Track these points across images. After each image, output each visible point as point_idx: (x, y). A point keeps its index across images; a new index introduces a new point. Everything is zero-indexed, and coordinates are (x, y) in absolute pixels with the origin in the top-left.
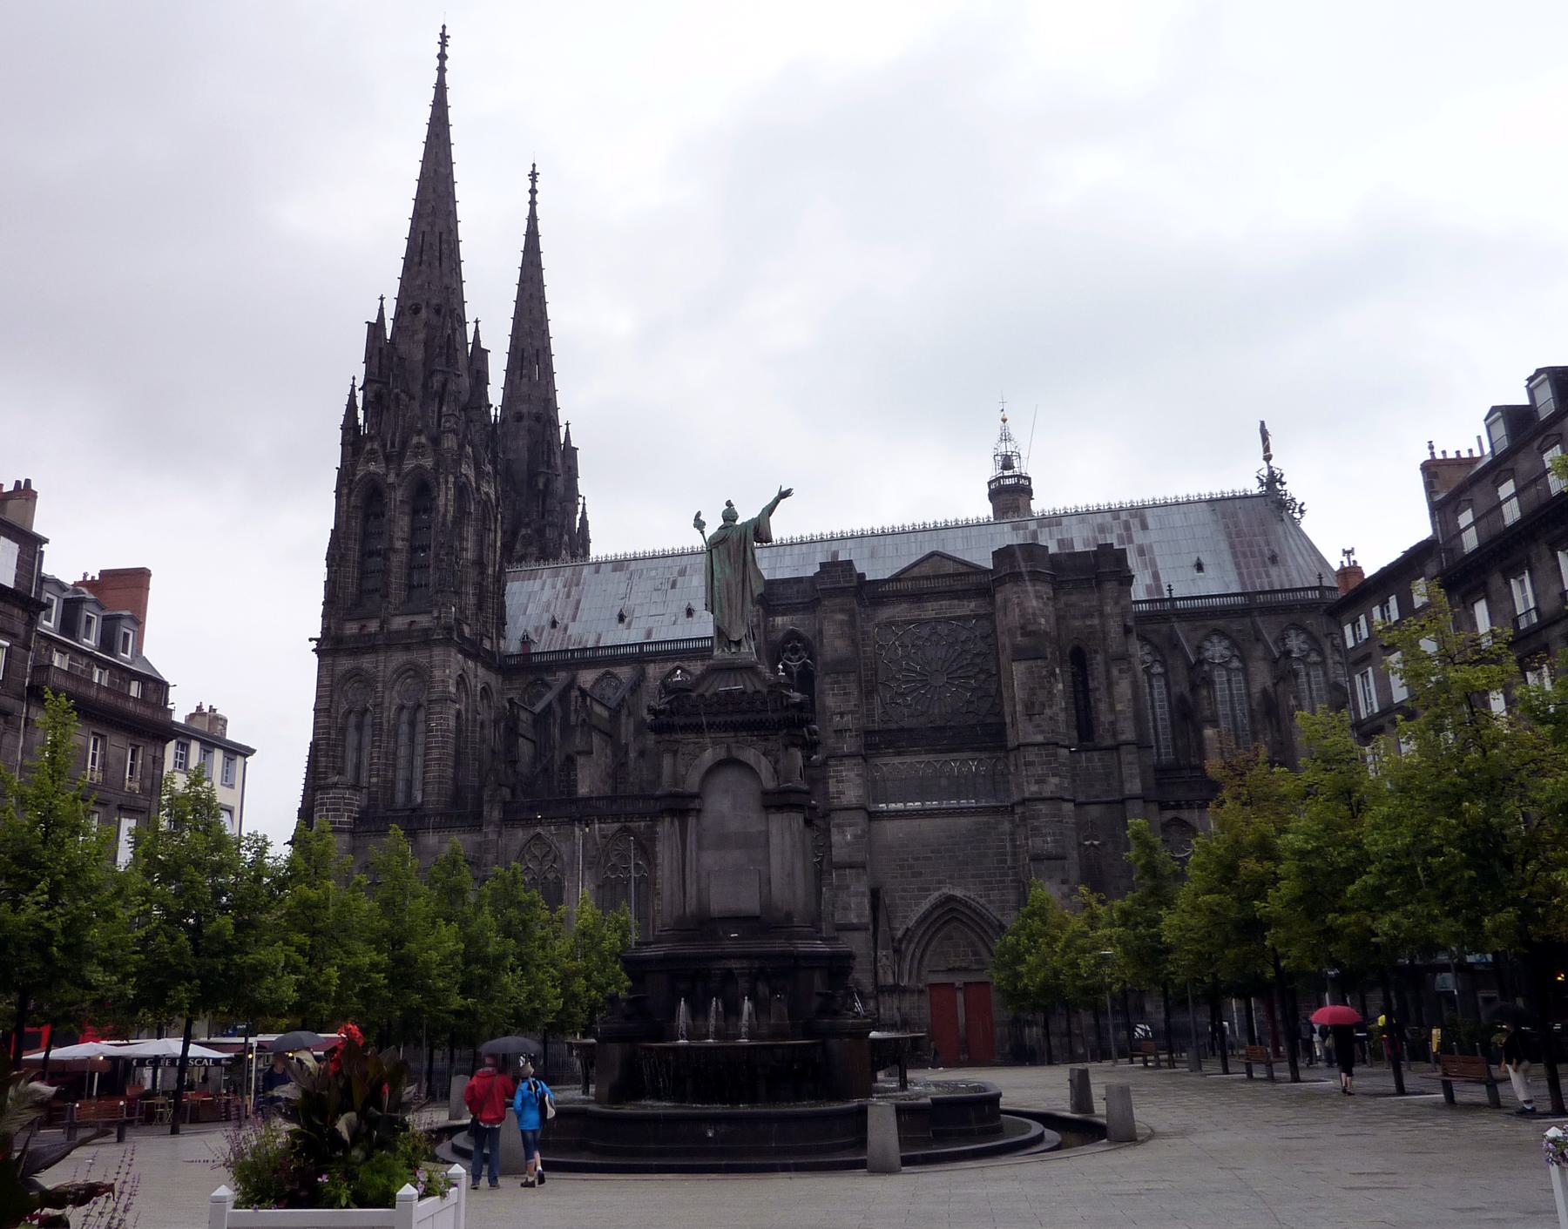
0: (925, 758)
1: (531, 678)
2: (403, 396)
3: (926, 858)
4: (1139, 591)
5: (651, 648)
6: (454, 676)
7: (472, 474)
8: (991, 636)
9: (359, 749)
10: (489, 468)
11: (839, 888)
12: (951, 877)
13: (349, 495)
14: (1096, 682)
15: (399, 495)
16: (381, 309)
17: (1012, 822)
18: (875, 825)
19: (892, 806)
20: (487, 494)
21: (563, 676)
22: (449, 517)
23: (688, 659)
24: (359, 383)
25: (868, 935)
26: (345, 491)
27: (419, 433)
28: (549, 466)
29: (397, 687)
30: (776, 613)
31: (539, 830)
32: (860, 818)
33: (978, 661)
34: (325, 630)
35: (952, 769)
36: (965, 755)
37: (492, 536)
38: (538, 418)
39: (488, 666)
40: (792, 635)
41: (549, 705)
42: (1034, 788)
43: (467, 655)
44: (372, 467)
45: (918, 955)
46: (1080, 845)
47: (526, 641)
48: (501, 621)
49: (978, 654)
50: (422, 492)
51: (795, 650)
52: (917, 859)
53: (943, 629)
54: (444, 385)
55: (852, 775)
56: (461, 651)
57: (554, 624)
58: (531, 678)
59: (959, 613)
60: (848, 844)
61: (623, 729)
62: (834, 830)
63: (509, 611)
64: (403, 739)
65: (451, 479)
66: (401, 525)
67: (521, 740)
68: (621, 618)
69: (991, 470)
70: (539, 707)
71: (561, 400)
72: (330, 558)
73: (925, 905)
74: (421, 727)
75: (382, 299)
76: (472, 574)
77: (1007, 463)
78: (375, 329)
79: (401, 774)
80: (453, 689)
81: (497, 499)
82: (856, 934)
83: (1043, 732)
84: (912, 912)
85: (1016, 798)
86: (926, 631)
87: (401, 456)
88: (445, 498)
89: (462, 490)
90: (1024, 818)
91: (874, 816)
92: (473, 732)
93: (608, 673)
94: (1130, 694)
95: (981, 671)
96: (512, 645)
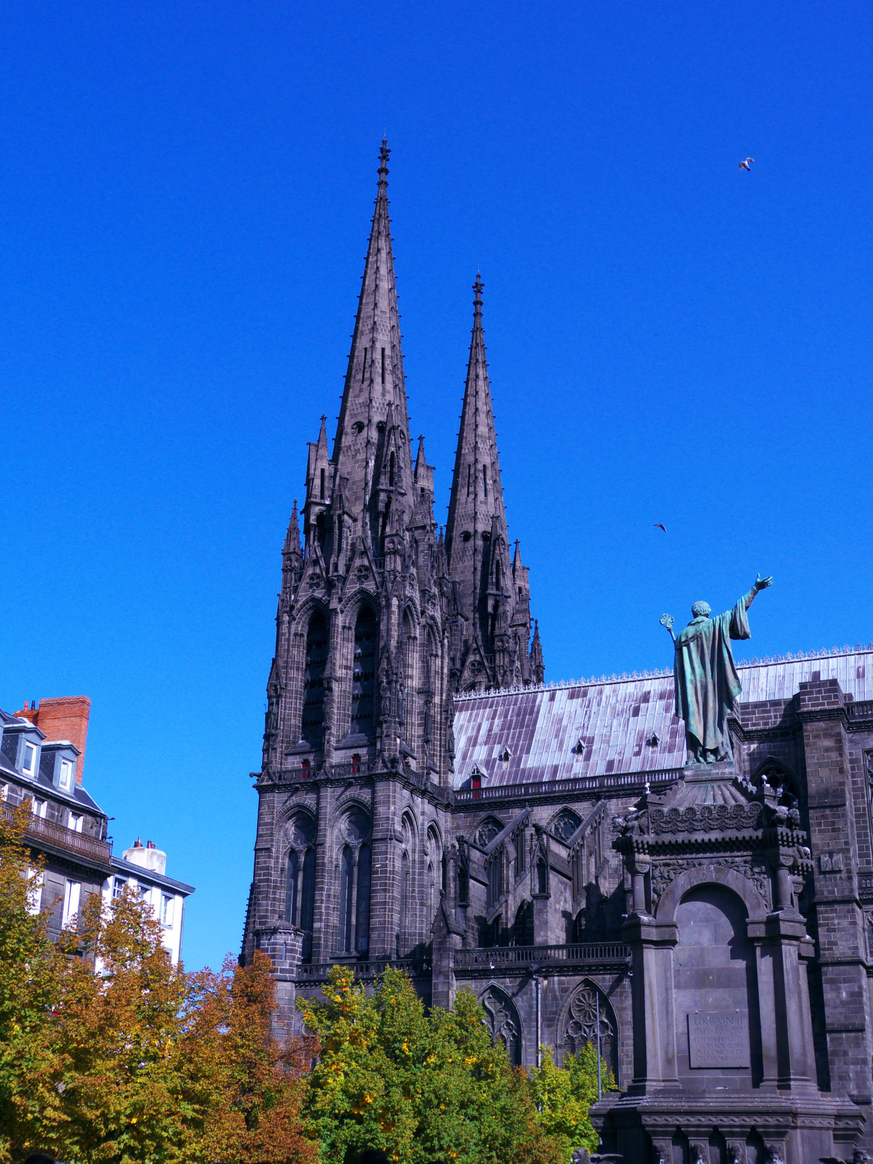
1: (483, 815)
2: (346, 517)
6: (400, 813)
7: (417, 596)
10: (435, 590)
11: (835, 1053)
20: (433, 618)
21: (517, 813)
24: (301, 506)
28: (498, 586)
31: (493, 982)
37: (438, 661)
38: (486, 537)
41: (502, 844)
54: (388, 505)
56: (406, 785)
58: (483, 815)
60: (843, 1004)
61: (584, 872)
66: (344, 654)
70: (491, 846)
80: (398, 827)
81: (443, 623)
87: (344, 580)
89: (406, 614)
92: (421, 874)
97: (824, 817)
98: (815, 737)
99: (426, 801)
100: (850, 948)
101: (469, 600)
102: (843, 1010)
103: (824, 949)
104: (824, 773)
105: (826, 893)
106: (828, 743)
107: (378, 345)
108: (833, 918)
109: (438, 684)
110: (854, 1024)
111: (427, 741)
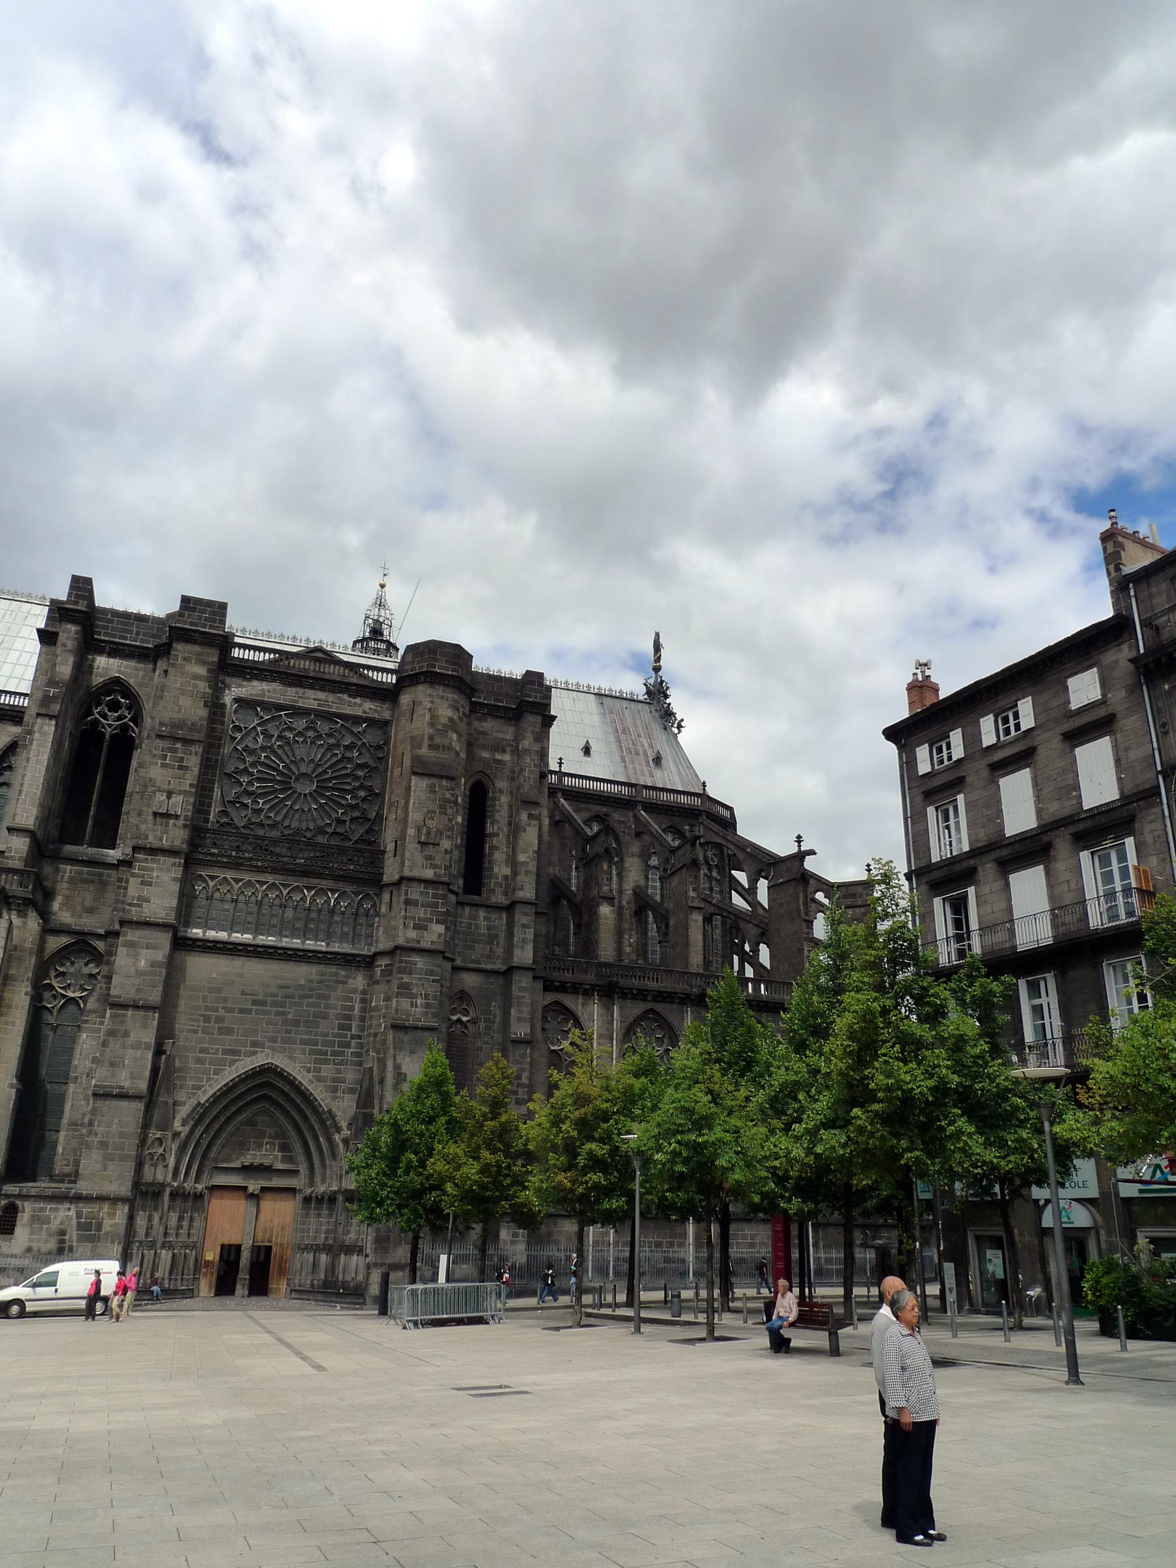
0: (270, 879)
3: (241, 1011)
8: (381, 751)
12: (273, 1040)
14: (497, 824)
17: (371, 977)
18: (180, 955)
19: (211, 934)
25: (140, 1106)
30: (101, 652)
33: (360, 773)
35: (303, 899)
36: (325, 884)
40: (116, 685)
51: (114, 706)
52: (231, 1010)
53: (323, 727)
55: (166, 877)
59: (348, 711)
60: (139, 974)
62: (122, 951)
73: (229, 1074)
82: (124, 1104)
83: (434, 866)
84: (203, 1083)
86: (301, 724)
90: (388, 972)
91: (182, 944)
94: (520, 853)
95: (362, 787)
97: (174, 751)
98: (185, 659)
100: (165, 909)
102: (136, 981)
103: (131, 905)
104: (185, 702)
105: (151, 839)
106: (201, 670)
108: (152, 870)
110: (146, 1000)
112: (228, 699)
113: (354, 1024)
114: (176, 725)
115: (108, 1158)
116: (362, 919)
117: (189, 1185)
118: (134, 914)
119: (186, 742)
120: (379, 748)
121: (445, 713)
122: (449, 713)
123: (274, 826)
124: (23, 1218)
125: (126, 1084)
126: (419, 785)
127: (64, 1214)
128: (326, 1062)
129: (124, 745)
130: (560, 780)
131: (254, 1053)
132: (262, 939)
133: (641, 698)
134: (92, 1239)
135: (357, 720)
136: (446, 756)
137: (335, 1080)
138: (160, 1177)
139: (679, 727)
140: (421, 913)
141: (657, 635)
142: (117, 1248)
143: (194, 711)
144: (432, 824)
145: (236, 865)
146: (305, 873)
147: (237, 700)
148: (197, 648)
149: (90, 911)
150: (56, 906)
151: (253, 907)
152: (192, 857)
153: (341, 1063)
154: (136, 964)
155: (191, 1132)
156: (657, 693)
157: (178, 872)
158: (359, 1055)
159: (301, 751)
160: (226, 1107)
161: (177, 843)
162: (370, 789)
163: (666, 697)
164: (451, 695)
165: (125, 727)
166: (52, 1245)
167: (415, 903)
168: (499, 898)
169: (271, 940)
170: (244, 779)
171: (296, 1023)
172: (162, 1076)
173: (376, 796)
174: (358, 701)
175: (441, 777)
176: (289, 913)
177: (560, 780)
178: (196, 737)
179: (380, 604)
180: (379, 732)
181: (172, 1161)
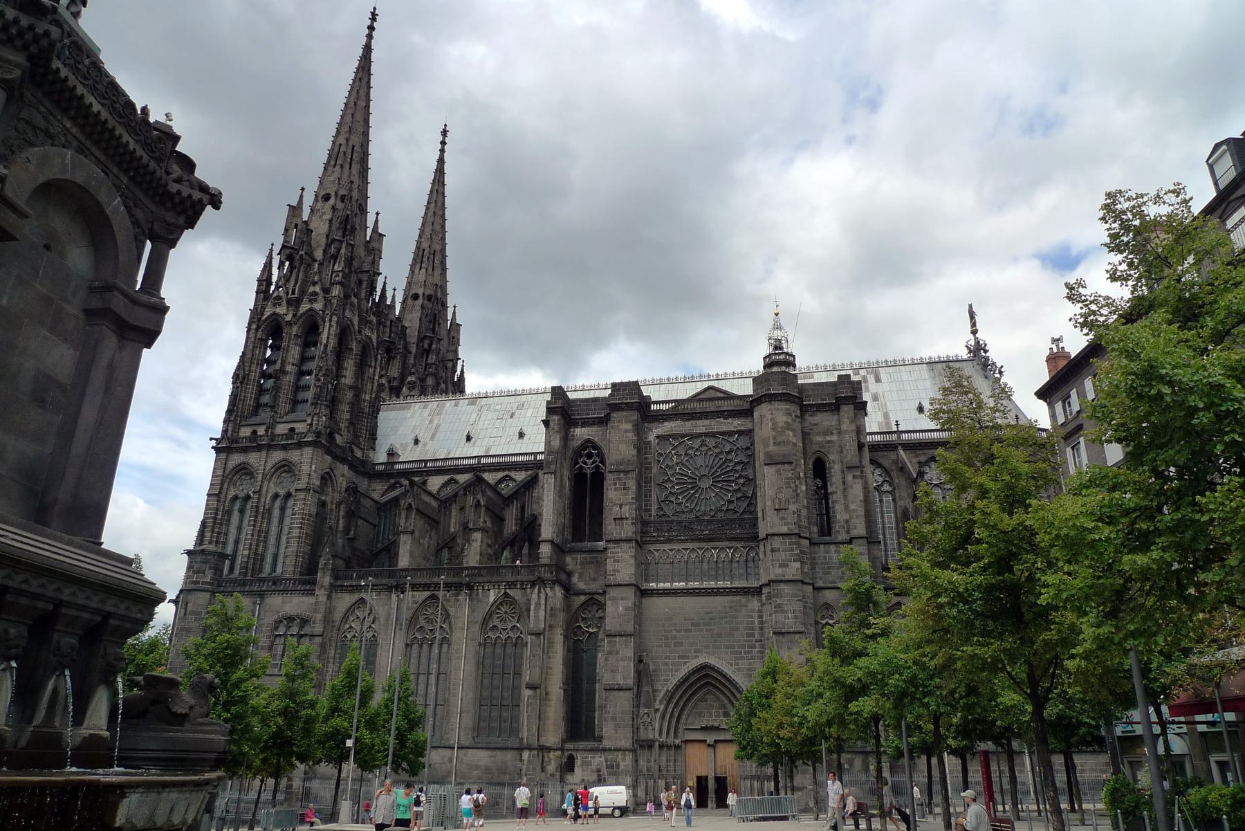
0: (690, 545)
1: (392, 481)
3: (686, 631)
4: (873, 423)
5: (490, 460)
8: (750, 450)
9: (240, 528)
10: (374, 319)
11: (610, 653)
12: (707, 647)
13: (257, 330)
14: (834, 486)
15: (295, 330)
16: (301, 197)
19: (661, 585)
22: (330, 348)
23: (515, 470)
24: (277, 249)
25: (628, 695)
26: (254, 326)
27: (315, 284)
28: (433, 331)
29: (274, 479)
30: (576, 425)
32: (630, 593)
33: (738, 468)
34: (225, 431)
37: (371, 370)
38: (429, 298)
39: (352, 467)
40: (588, 443)
42: (779, 571)
43: (335, 457)
44: (278, 310)
45: (676, 714)
46: (817, 623)
47: (391, 454)
48: (373, 437)
49: (737, 463)
50: (311, 329)
51: (589, 456)
53: (711, 442)
55: (626, 556)
57: (416, 442)
58: (392, 481)
59: (724, 429)
62: (609, 603)
63: (380, 432)
64: (275, 520)
65: (335, 319)
67: (360, 522)
68: (469, 438)
69: (766, 349)
71: (450, 288)
72: (236, 377)
73: (684, 671)
74: (289, 512)
75: (303, 189)
76: (349, 395)
77: (778, 347)
78: (295, 210)
79: (271, 550)
82: (621, 694)
83: (787, 524)
84: (670, 677)
85: (764, 580)
86: (697, 443)
88: (328, 334)
90: (769, 597)
91: (645, 593)
93: (452, 479)
95: (741, 476)
96: (381, 457)
99: (346, 467)
101: (415, 340)
104: (623, 448)
107: (351, 143)
109: (369, 386)
111: (351, 423)
112: (651, 437)
113: (756, 633)
114: (618, 464)
115: (617, 726)
116: (750, 563)
117: (670, 741)
118: (612, 580)
119: (626, 472)
120: (748, 448)
121: (782, 419)
122: (784, 419)
123: (691, 511)
124: (578, 763)
125: (621, 682)
126: (769, 472)
127: (598, 760)
128: (742, 658)
129: (599, 477)
130: (899, 437)
131: (697, 657)
132: (691, 585)
133: (965, 357)
134: (615, 774)
135: (731, 433)
136: (786, 449)
137: (749, 670)
138: (651, 736)
139: (1001, 373)
140: (782, 556)
141: (970, 306)
142: (629, 780)
143: (629, 452)
144: (781, 496)
145: (669, 541)
146: (711, 540)
147: (658, 437)
148: (625, 413)
149: (594, 580)
150: (575, 579)
151: (683, 565)
152: (640, 544)
153: (752, 658)
154: (618, 609)
155: (666, 708)
156: (978, 350)
157: (632, 552)
158: (762, 652)
159: (700, 461)
160: (686, 691)
161: (630, 534)
162: (746, 477)
163: (986, 352)
164: (783, 406)
165: (597, 467)
166: (594, 778)
167: (779, 550)
168: (843, 536)
169: (697, 584)
170: (668, 485)
171: (720, 635)
172: (642, 674)
173: (751, 481)
174: (730, 420)
175: (783, 463)
176: (705, 566)
177: (899, 437)
178: (631, 468)
179: (778, 327)
180: (747, 438)
181: (657, 727)
